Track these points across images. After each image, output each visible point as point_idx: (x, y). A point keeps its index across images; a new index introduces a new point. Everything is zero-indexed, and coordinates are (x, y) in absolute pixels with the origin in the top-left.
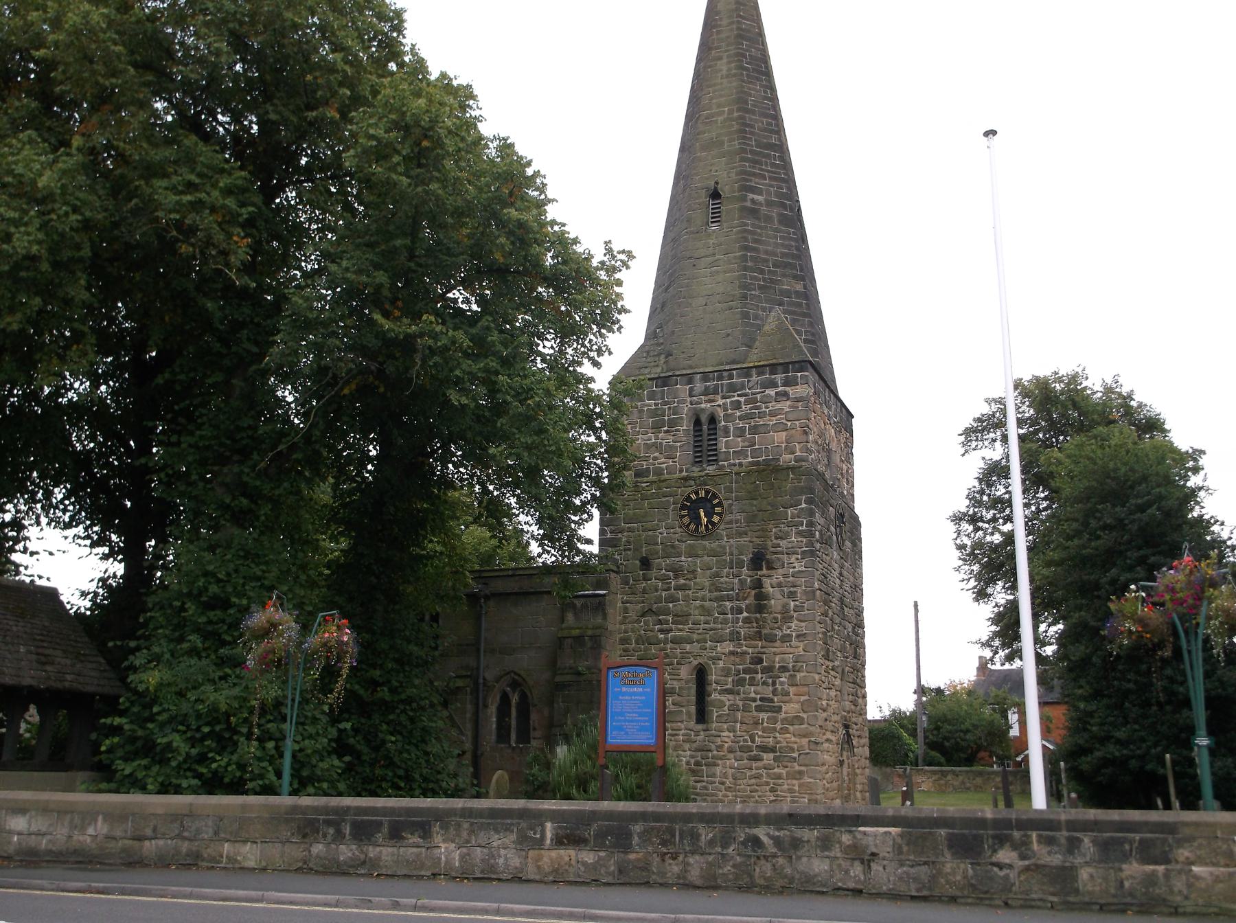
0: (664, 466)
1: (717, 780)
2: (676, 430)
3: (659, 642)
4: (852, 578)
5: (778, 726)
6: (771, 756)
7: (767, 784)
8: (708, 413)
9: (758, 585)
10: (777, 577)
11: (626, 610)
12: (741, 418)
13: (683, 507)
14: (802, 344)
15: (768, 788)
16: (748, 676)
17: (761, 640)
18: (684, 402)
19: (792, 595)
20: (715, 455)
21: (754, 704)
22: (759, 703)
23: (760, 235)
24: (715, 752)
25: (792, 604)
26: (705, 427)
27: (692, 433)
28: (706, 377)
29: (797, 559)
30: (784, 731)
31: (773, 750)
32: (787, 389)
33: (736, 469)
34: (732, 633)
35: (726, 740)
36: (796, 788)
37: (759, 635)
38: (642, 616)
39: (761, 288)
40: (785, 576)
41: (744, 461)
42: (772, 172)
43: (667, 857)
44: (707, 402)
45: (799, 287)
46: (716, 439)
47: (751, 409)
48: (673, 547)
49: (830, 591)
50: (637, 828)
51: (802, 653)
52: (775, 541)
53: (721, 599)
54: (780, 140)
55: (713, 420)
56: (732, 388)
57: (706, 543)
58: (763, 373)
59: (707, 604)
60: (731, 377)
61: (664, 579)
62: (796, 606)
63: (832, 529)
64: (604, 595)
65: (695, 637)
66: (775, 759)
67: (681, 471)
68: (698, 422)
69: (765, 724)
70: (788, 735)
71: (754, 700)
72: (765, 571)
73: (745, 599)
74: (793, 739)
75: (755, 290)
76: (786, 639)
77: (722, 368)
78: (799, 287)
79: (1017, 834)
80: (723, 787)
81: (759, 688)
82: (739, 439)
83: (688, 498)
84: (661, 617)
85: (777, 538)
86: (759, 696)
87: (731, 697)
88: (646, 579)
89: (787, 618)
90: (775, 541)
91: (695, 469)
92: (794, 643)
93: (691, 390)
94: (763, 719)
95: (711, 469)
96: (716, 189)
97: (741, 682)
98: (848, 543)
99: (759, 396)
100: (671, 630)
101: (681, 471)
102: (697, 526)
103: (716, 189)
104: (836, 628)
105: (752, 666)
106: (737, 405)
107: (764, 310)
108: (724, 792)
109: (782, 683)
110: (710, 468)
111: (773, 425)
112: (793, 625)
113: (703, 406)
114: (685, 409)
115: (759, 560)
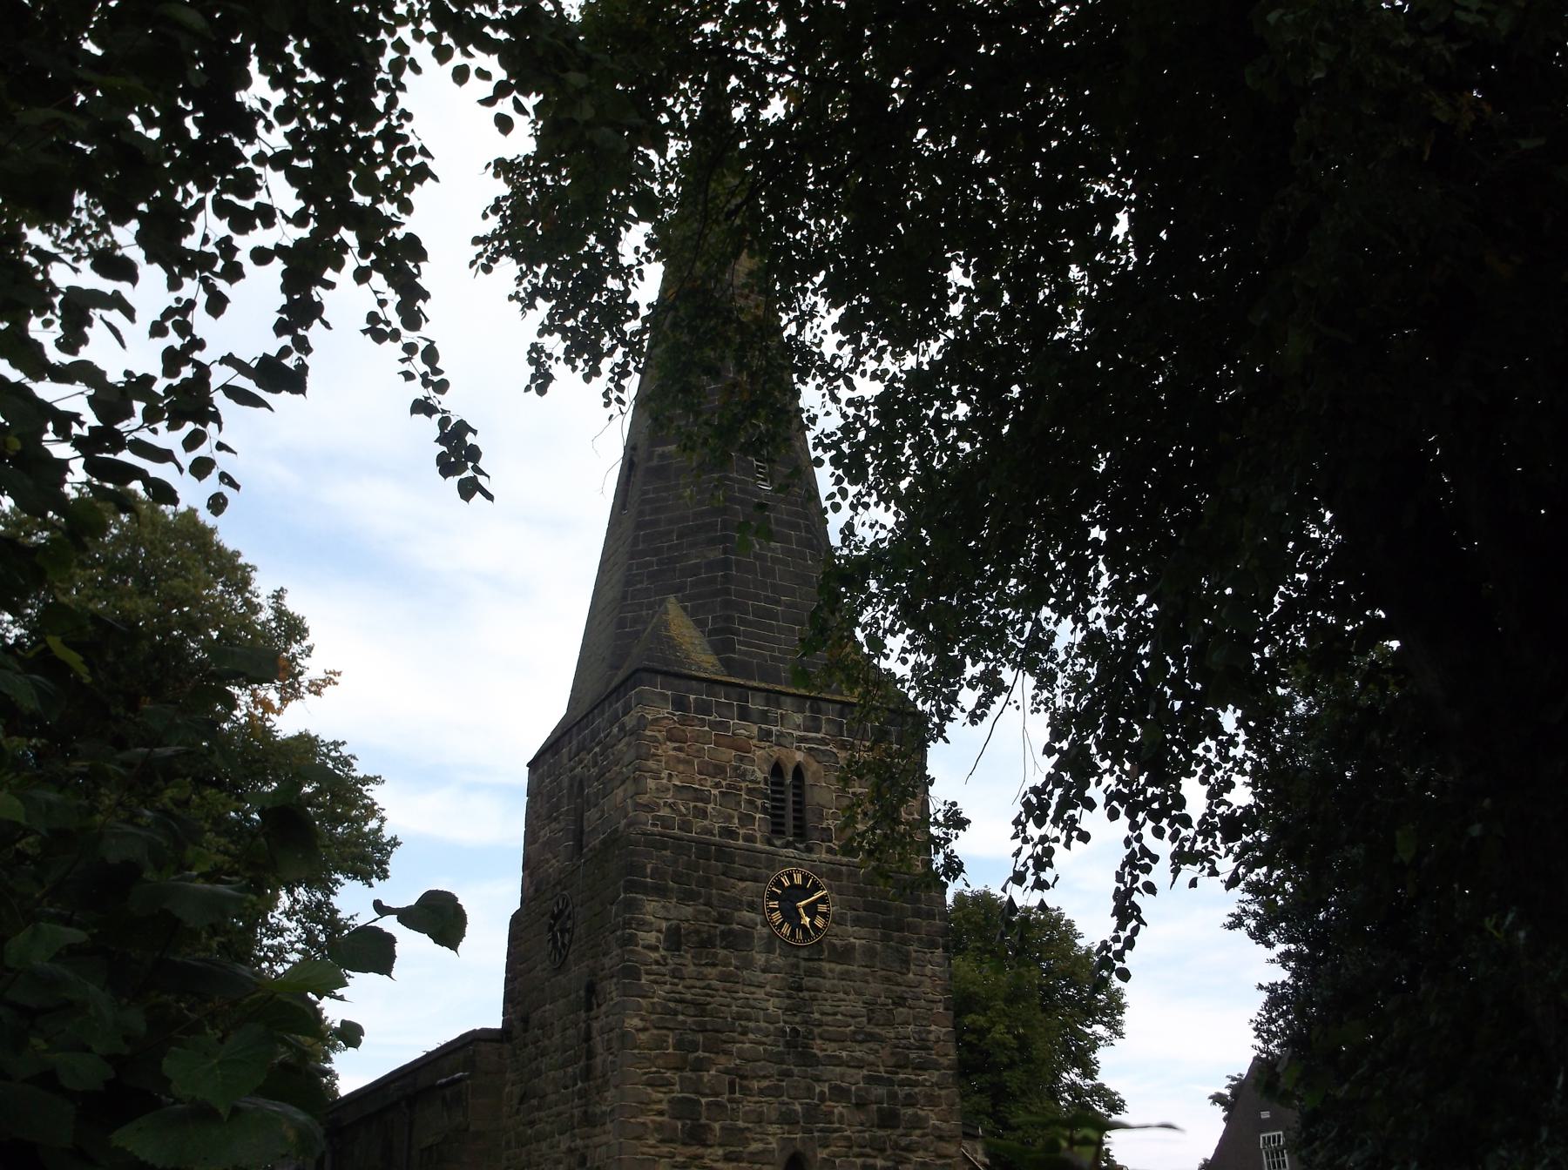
8: (578, 779)
53: (563, 1066)
64: (460, 1080)
72: (593, 1014)
75: (641, 582)
107: (650, 606)
114: (566, 783)
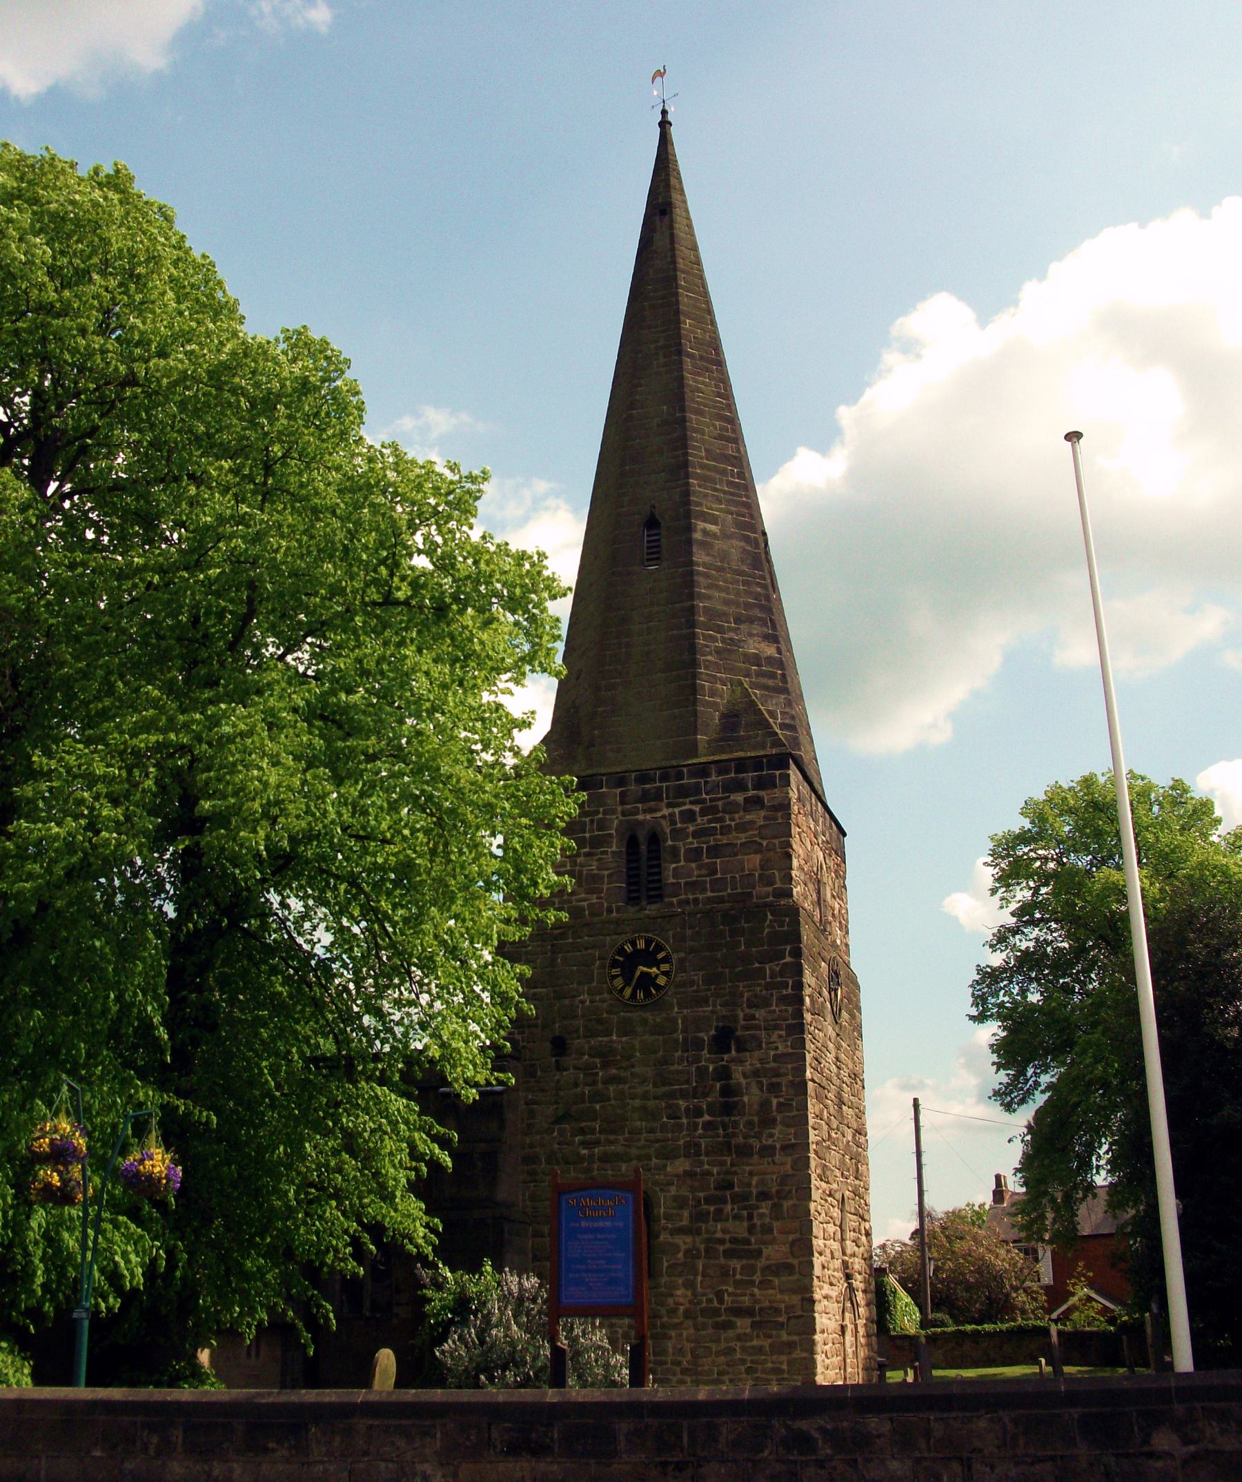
0: (585, 904)
1: (669, 1359)
2: (602, 853)
3: (581, 1159)
4: (851, 1065)
5: (757, 1278)
6: (748, 1321)
7: (743, 1361)
9: (724, 1074)
10: (752, 1061)
11: (532, 1114)
12: (696, 834)
13: (615, 964)
14: (779, 731)
15: (743, 1368)
16: (712, 1209)
17: (730, 1154)
18: (613, 812)
19: (774, 1088)
21: (721, 1248)
22: (728, 1245)
23: (716, 579)
24: (665, 1319)
25: (775, 1101)
26: (643, 848)
27: (624, 856)
28: (643, 778)
29: (780, 1036)
30: (764, 1284)
31: (749, 1312)
32: (762, 793)
34: (687, 1145)
35: (681, 1300)
36: (785, 1367)
37: (727, 1147)
38: (558, 1120)
39: (718, 652)
40: (762, 1061)
42: (732, 494)
43: (670, 1468)
44: (644, 811)
45: (770, 651)
46: (659, 866)
47: (709, 821)
48: (600, 1021)
49: (825, 1083)
50: (623, 1427)
51: (790, 1172)
52: (747, 1011)
54: (738, 451)
55: (655, 838)
56: (683, 792)
57: (648, 1015)
58: (727, 771)
59: (651, 1104)
61: (588, 1069)
62: (779, 1104)
63: (825, 993)
65: (634, 1151)
66: (754, 1325)
67: (610, 911)
68: (632, 843)
69: (738, 1277)
70: (771, 1291)
71: (722, 1241)
73: (705, 1095)
74: (779, 1296)
75: (710, 654)
76: (768, 1151)
77: (668, 764)
78: (770, 651)
79: (1179, 1409)
80: (678, 1369)
81: (730, 1225)
82: (693, 865)
83: (621, 951)
84: (583, 1124)
85: (749, 1007)
86: (727, 1237)
87: (689, 1239)
88: (559, 1067)
89: (768, 1122)
90: (747, 1011)
92: (777, 1158)
93: (623, 794)
94: (734, 1270)
95: (652, 909)
96: (652, 514)
97: (700, 1217)
98: (844, 1014)
99: (720, 803)
100: (598, 1143)
101: (610, 911)
103: (652, 514)
104: (833, 1135)
105: (718, 1193)
106: (689, 816)
108: (680, 1376)
109: (762, 1216)
110: (654, 907)
111: (742, 844)
112: (776, 1131)
113: (640, 817)
115: (724, 1039)
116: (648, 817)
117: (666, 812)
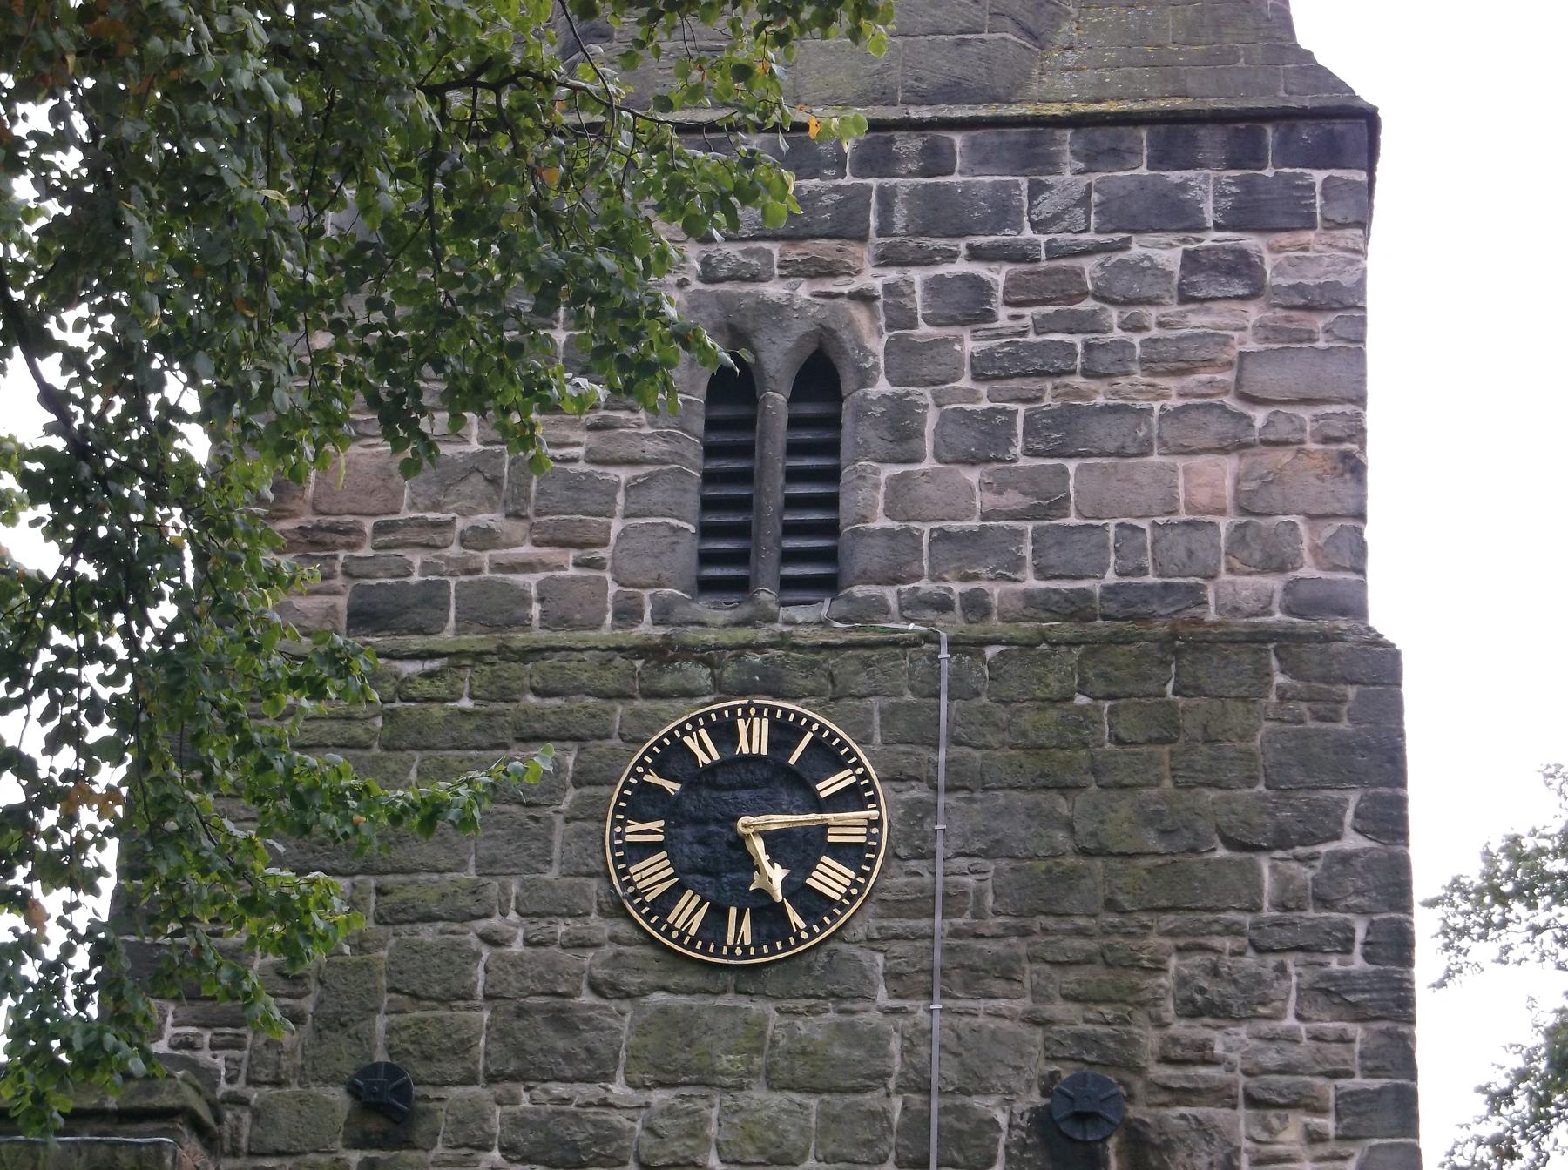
20: (829, 556)
33: (949, 626)
41: (996, 590)
44: (792, 270)
48: (562, 1020)
60: (936, 161)
91: (703, 608)
102: (717, 916)
116: (804, 290)
117: (874, 279)
